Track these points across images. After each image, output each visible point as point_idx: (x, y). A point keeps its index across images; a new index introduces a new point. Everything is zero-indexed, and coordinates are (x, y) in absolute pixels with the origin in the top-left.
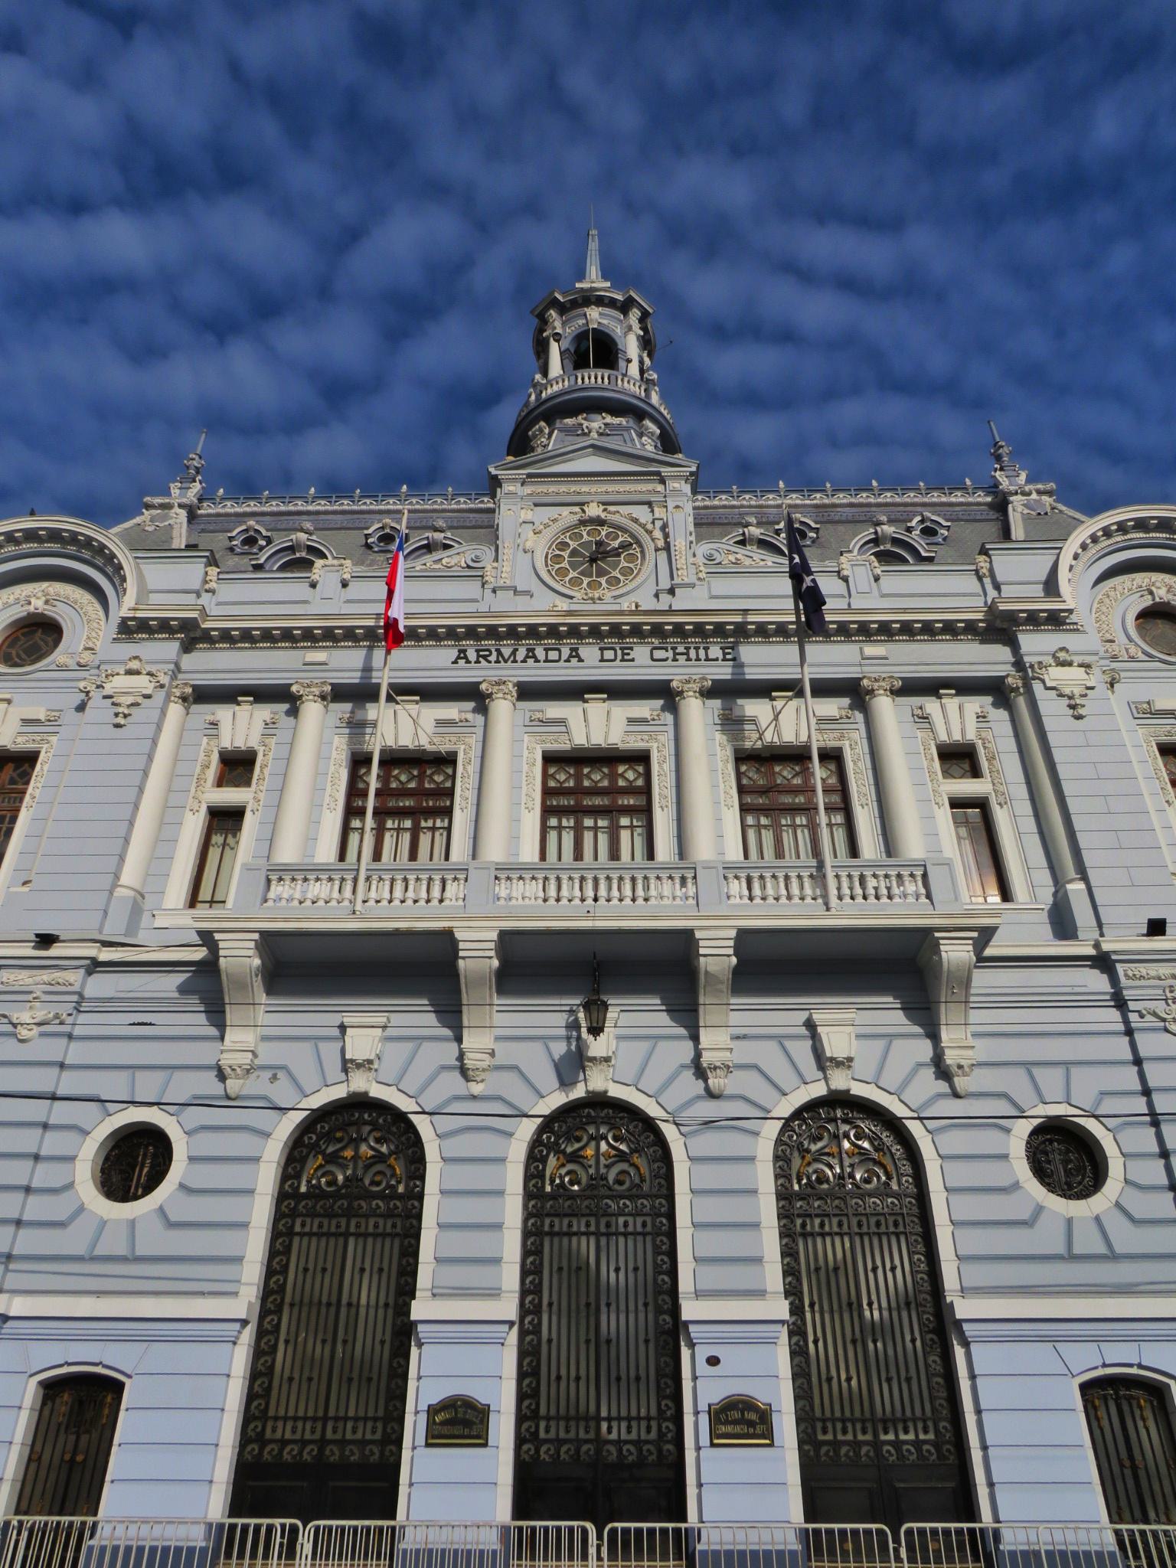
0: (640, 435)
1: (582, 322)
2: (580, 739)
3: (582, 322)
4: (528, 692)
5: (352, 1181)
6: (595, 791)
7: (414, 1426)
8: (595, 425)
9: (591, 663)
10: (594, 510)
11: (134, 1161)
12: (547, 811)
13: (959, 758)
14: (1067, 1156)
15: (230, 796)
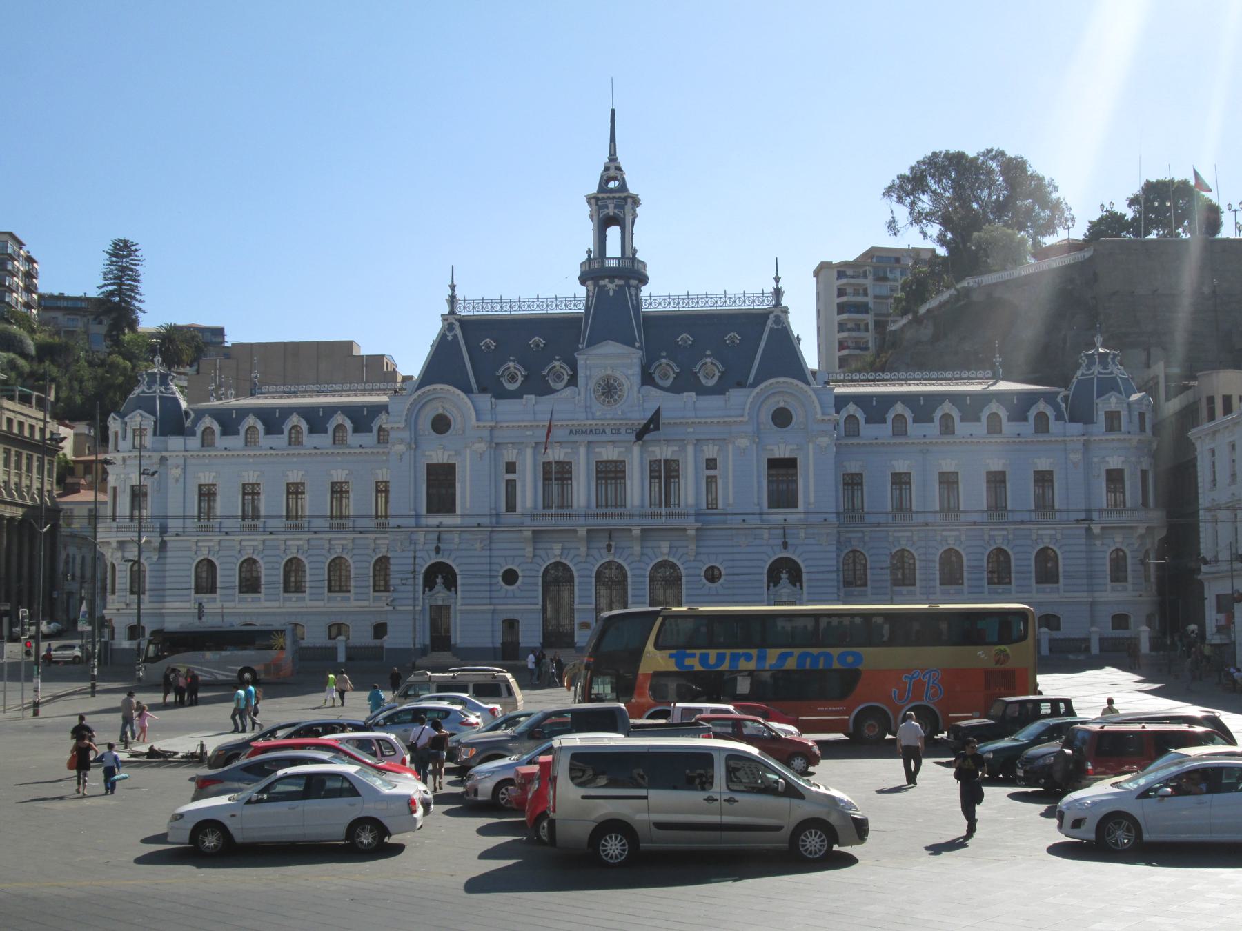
0: (629, 287)
1: (606, 211)
2: (605, 458)
3: (606, 211)
4: (589, 442)
5: (557, 579)
6: (610, 473)
7: (576, 627)
8: (611, 286)
9: (609, 437)
10: (609, 372)
11: (510, 577)
12: (598, 478)
13: (711, 463)
14: (712, 575)
15: (511, 477)
